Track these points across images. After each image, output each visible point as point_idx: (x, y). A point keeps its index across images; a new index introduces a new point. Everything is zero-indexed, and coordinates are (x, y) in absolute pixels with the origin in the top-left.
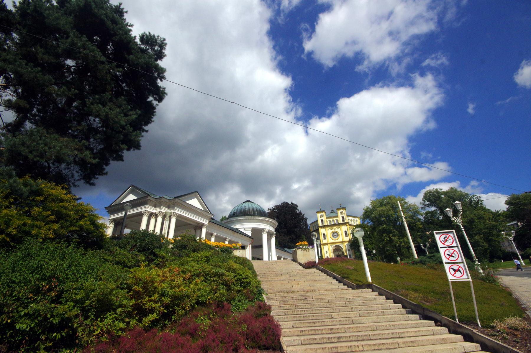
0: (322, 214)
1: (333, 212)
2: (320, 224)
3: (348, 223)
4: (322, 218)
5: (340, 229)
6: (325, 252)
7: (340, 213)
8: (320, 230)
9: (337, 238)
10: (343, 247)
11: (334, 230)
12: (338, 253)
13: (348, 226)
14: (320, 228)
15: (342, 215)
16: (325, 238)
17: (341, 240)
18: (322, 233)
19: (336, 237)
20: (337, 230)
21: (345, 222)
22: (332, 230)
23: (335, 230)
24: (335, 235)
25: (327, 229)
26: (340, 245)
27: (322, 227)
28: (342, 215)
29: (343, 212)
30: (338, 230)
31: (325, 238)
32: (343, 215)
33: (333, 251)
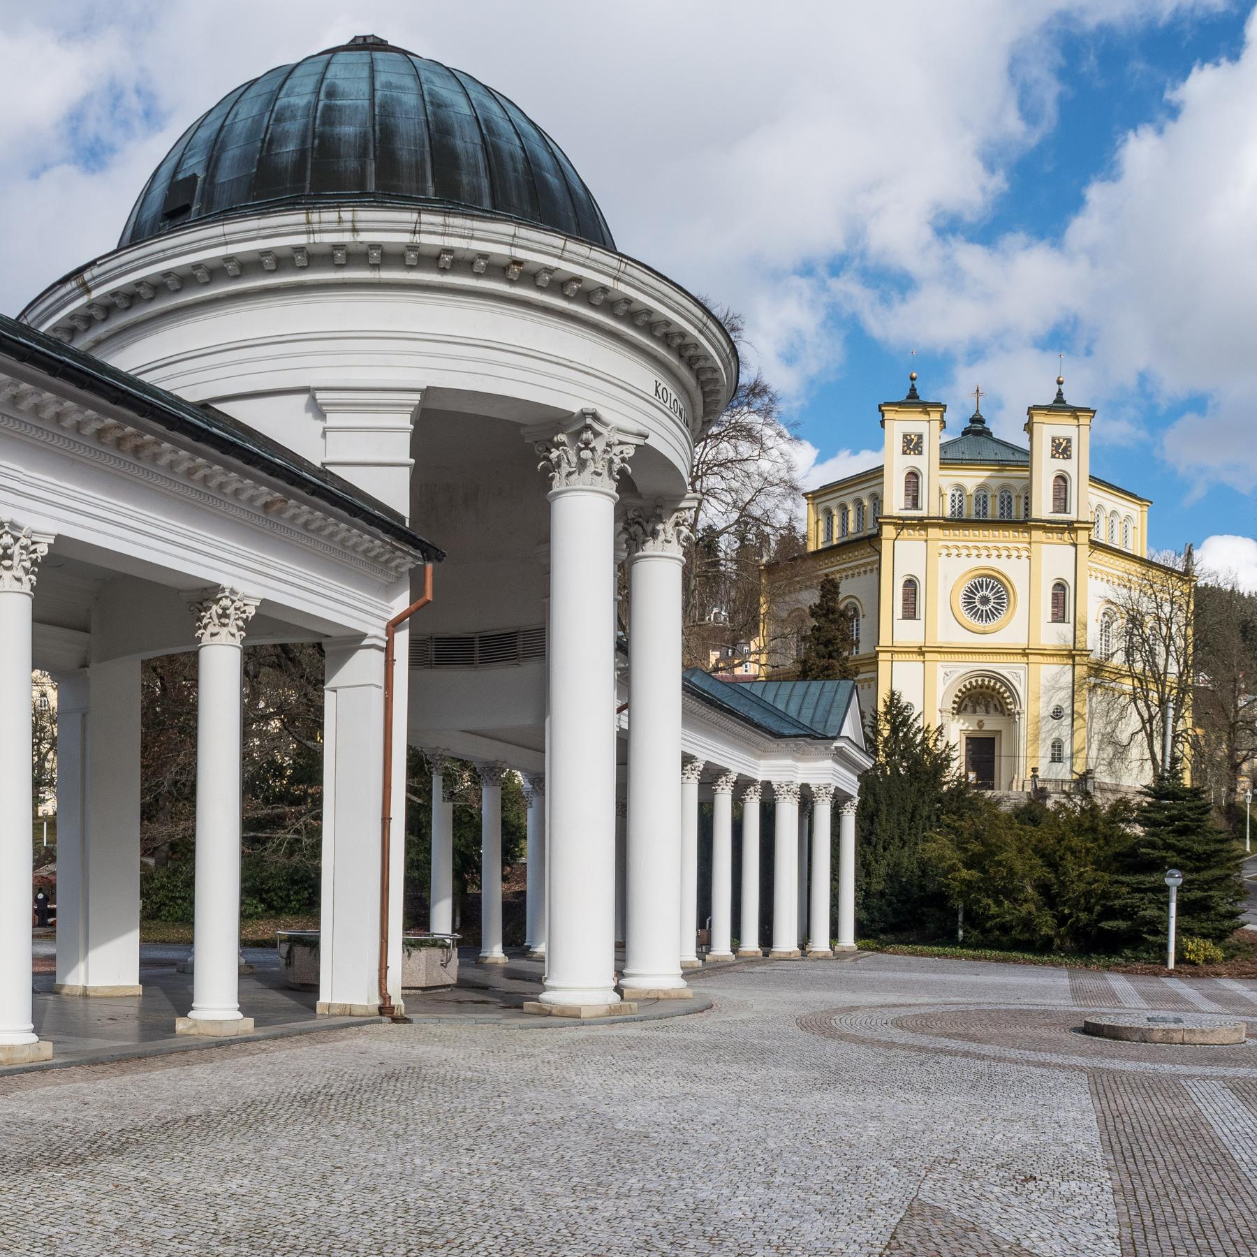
1: (978, 433)
2: (895, 502)
3: (1089, 526)
5: (1024, 561)
8: (886, 546)
10: (1021, 690)
11: (984, 562)
12: (981, 724)
13: (1084, 550)
14: (888, 531)
15: (1061, 464)
16: (910, 612)
21: (1072, 517)
22: (974, 563)
23: (994, 563)
24: (985, 600)
26: (1006, 668)
27: (902, 524)
30: (1013, 570)
31: (910, 612)
32: (1069, 466)
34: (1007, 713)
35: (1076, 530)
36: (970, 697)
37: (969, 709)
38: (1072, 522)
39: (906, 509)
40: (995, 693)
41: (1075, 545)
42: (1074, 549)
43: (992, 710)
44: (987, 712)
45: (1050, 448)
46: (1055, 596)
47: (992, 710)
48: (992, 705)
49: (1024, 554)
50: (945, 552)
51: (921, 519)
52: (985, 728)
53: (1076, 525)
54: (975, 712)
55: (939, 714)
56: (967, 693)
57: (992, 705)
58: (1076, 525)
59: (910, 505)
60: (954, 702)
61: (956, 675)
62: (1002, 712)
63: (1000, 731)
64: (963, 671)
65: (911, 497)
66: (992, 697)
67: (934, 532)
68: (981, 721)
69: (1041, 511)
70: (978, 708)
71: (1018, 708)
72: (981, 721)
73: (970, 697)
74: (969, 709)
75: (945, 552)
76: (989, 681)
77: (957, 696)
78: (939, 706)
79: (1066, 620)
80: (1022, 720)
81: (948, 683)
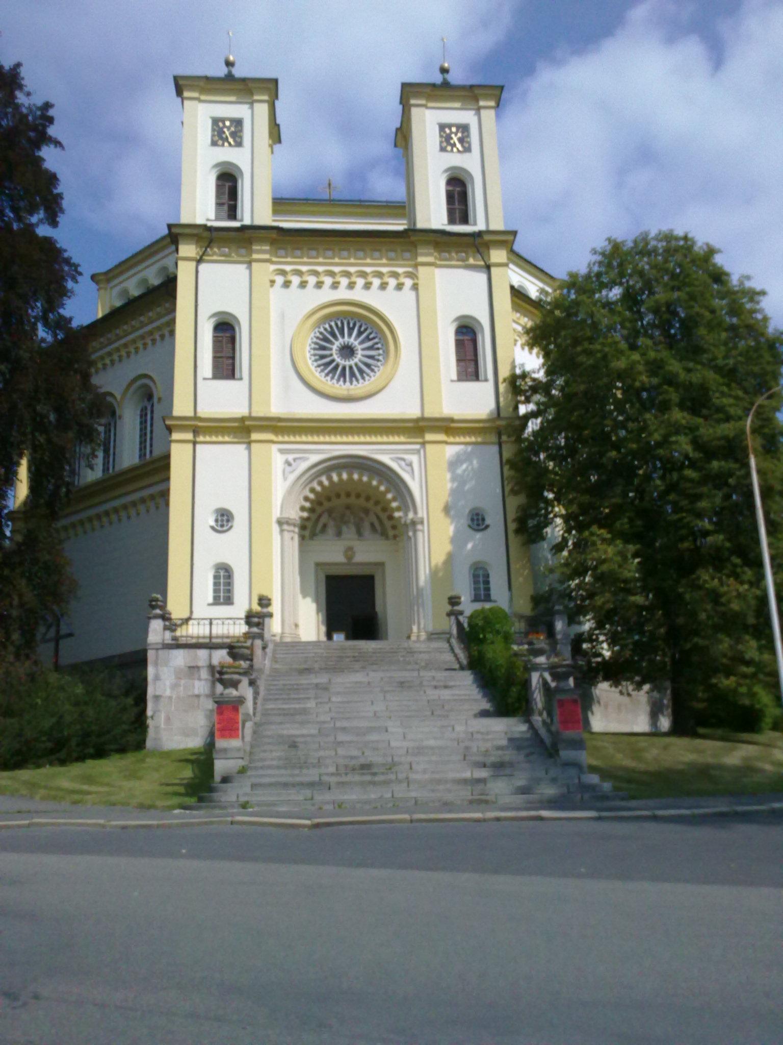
0: (240, 111)
4: (227, 154)
5: (408, 294)
6: (206, 519)
8: (185, 273)
9: (358, 387)
10: (414, 486)
12: (349, 552)
15: (455, 159)
17: (413, 412)
18: (211, 305)
19: (344, 374)
20: (374, 298)
23: (359, 295)
24: (347, 351)
25: (265, 270)
28: (455, 159)
29: (464, 128)
33: (295, 514)
34: (391, 533)
35: (488, 246)
36: (330, 512)
37: (331, 531)
38: (480, 234)
39: (218, 218)
40: (370, 505)
41: (488, 267)
43: (367, 532)
44: (359, 533)
45: (438, 139)
47: (367, 532)
48: (367, 525)
49: (408, 283)
50: (280, 280)
51: (244, 228)
54: (339, 534)
55: (276, 528)
56: (327, 505)
57: (367, 525)
58: (487, 238)
59: (225, 213)
60: (303, 509)
61: (304, 466)
62: (384, 534)
63: (381, 565)
64: (315, 458)
65: (226, 208)
66: (367, 511)
67: (261, 251)
69: (429, 220)
70: (344, 529)
71: (411, 515)
73: (330, 512)
74: (331, 531)
75: (280, 280)
77: (306, 499)
78: (276, 513)
79: (482, 376)
80: (420, 535)
81: (292, 477)
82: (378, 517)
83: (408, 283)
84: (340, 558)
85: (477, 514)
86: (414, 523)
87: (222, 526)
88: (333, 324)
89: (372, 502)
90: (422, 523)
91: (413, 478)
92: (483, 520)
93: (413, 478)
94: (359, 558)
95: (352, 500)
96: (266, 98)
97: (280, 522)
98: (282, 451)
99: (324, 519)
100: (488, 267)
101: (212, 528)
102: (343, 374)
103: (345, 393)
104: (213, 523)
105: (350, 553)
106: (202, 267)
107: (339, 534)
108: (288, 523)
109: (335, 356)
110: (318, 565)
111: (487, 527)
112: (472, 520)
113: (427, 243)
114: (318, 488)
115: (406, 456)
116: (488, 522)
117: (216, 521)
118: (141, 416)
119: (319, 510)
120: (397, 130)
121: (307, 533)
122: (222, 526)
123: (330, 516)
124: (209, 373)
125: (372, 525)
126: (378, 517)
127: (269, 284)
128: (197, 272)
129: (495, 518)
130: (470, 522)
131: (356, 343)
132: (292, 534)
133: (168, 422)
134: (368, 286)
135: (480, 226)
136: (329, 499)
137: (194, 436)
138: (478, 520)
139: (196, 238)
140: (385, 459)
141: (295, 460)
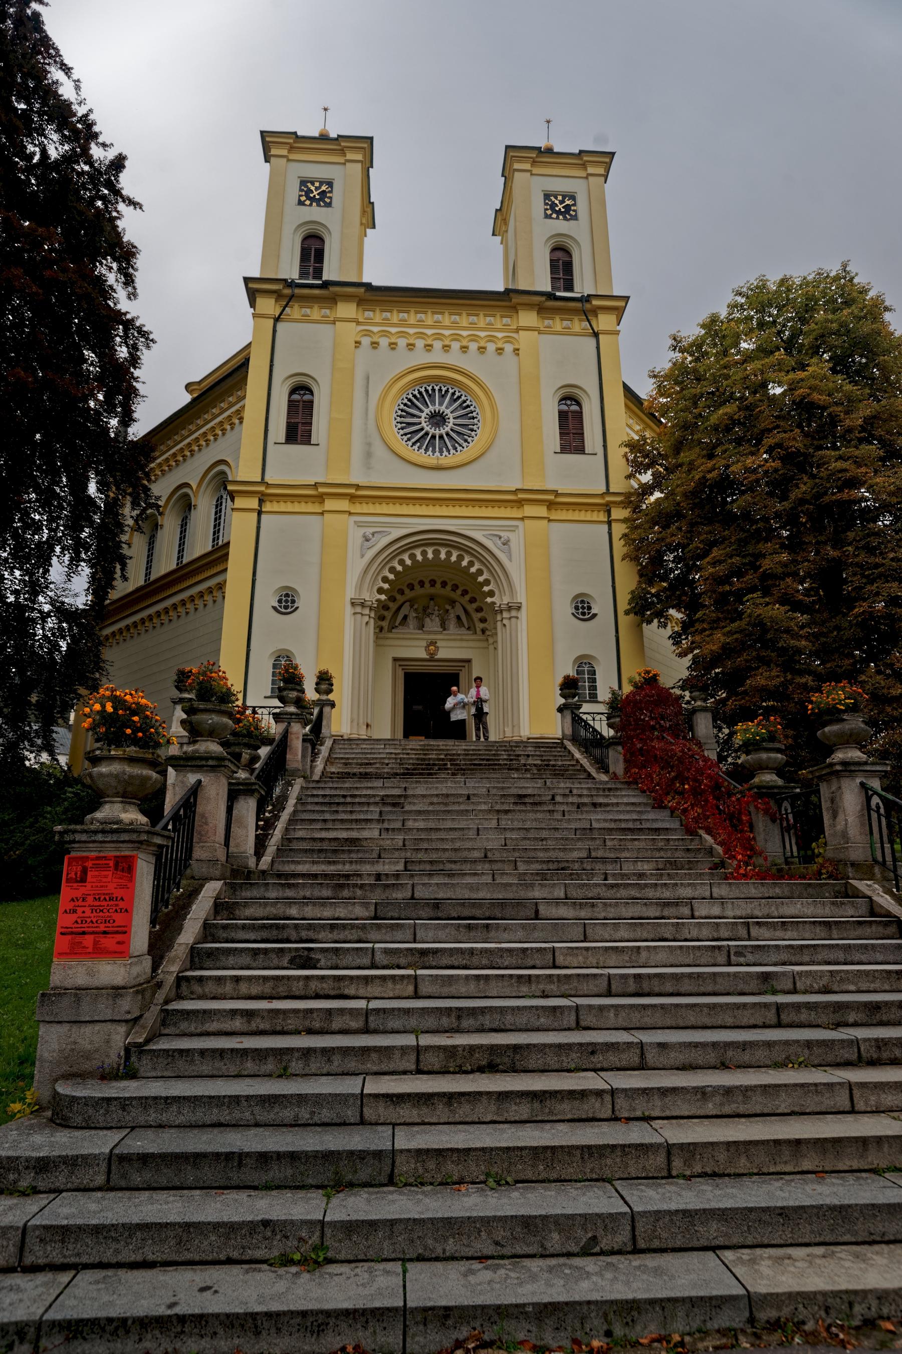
4: (315, 213)
6: (267, 599)
7: (539, 205)
11: (437, 356)
15: (560, 226)
20: (470, 363)
22: (420, 357)
24: (438, 419)
33: (371, 596)
34: (480, 626)
35: (595, 311)
37: (412, 622)
38: (588, 298)
41: (596, 335)
42: (593, 341)
43: (452, 624)
44: (444, 626)
46: (563, 416)
47: (452, 624)
49: (509, 348)
50: (366, 341)
52: (441, 655)
53: (595, 302)
55: (349, 610)
56: (409, 594)
57: (452, 615)
58: (595, 302)
60: (380, 591)
63: (469, 661)
66: (453, 602)
68: (433, 643)
70: (427, 620)
72: (433, 643)
73: (412, 602)
75: (366, 341)
76: (449, 554)
77: (385, 580)
78: (350, 593)
81: (370, 554)
82: (466, 611)
83: (509, 348)
84: (424, 655)
85: (582, 602)
86: (510, 608)
87: (286, 607)
88: (423, 390)
89: (459, 592)
90: (519, 608)
91: (510, 560)
92: (589, 608)
93: (510, 560)
94: (442, 654)
95: (438, 590)
96: (359, 157)
97: (353, 604)
98: (359, 525)
99: (405, 610)
100: (596, 335)
101: (274, 608)
102: (432, 443)
103: (435, 462)
104: (276, 604)
105: (432, 647)
106: (280, 326)
107: (421, 627)
108: (363, 605)
109: (423, 420)
110: (395, 660)
111: (595, 615)
112: (577, 608)
113: (529, 306)
114: (399, 568)
115: (502, 534)
116: (593, 611)
117: (280, 601)
118: (217, 506)
119: (400, 599)
120: (497, 210)
121: (385, 624)
122: (286, 607)
123: (412, 606)
124: (282, 437)
125: (458, 618)
126: (466, 611)
127: (354, 345)
128: (274, 331)
129: (602, 606)
130: (574, 611)
131: (448, 411)
132: (366, 619)
133: (230, 488)
134: (464, 349)
135: (588, 290)
136: (411, 587)
137: (260, 505)
138: (583, 608)
139: (275, 296)
140: (478, 536)
141: (373, 534)
